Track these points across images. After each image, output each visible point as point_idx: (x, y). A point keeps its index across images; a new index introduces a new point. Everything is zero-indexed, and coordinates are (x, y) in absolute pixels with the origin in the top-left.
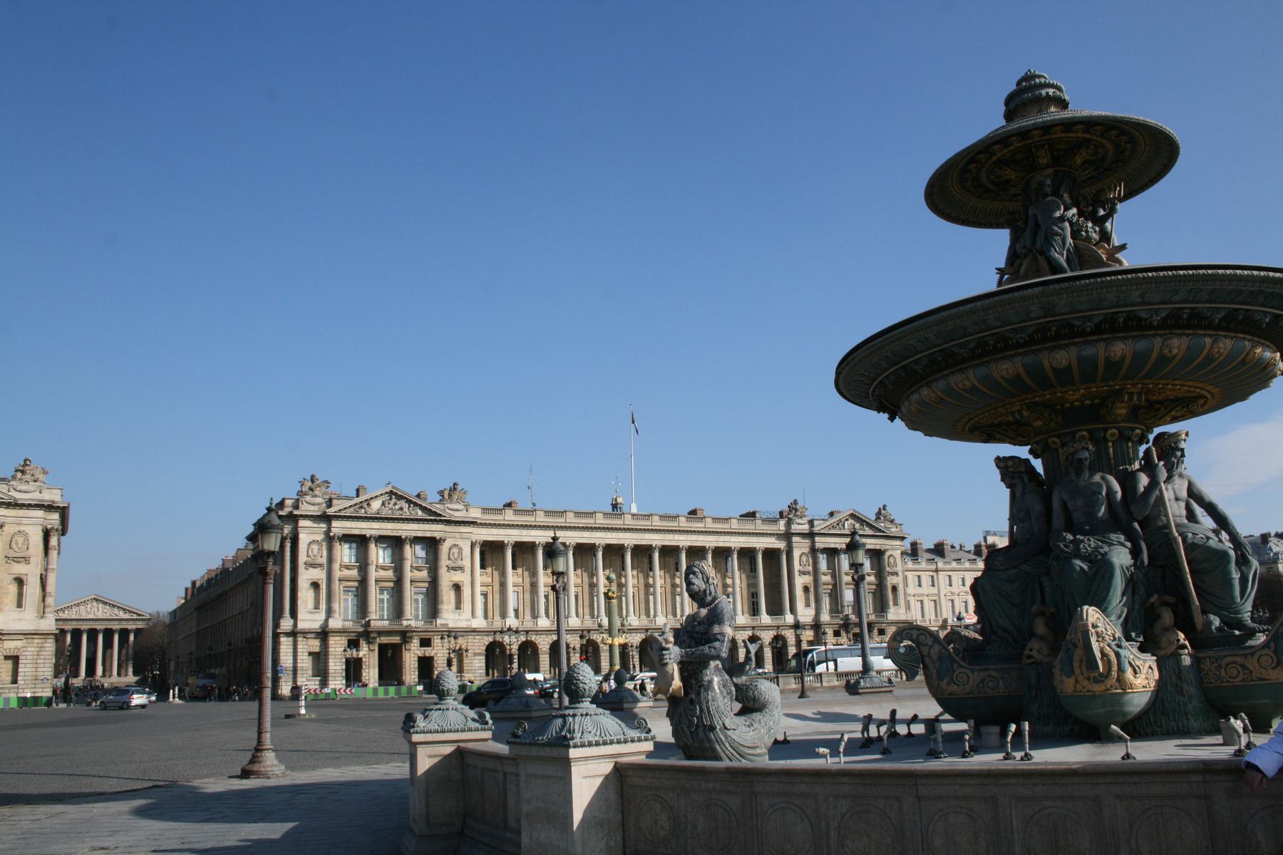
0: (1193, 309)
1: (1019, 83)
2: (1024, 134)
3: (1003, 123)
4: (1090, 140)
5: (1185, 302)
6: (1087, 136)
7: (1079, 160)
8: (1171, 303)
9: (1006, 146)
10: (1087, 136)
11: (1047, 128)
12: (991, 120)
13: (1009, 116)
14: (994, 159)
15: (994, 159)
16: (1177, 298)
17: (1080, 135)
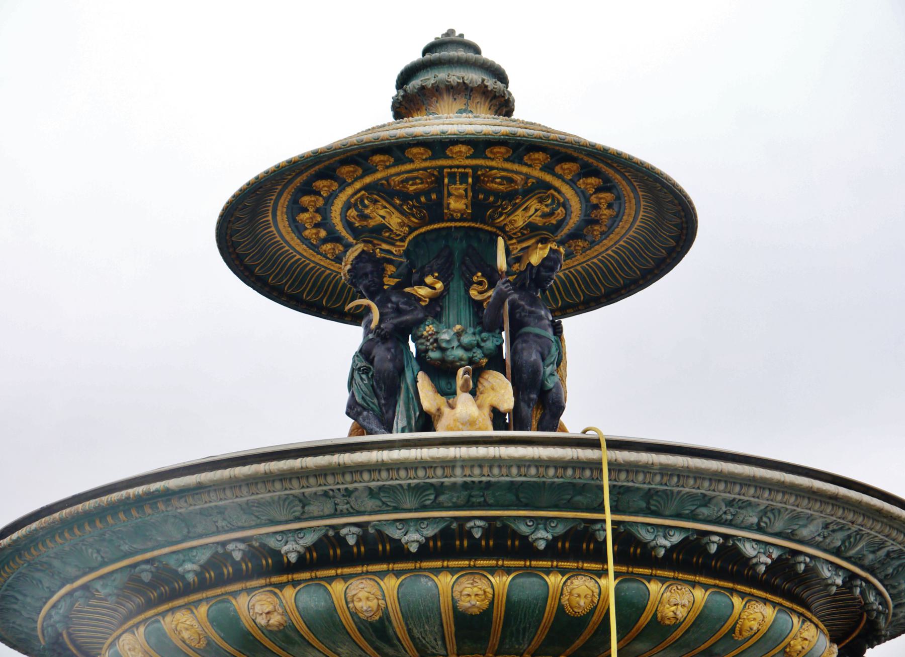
0: (726, 537)
1: (428, 50)
2: (438, 146)
3: (388, 116)
4: (549, 186)
5: (718, 522)
6: (548, 178)
7: (520, 219)
8: (693, 518)
9: (399, 161)
10: (548, 178)
11: (480, 145)
12: (362, 110)
13: (403, 107)
14: (368, 180)
15: (368, 180)
16: (705, 511)
17: (537, 173)
